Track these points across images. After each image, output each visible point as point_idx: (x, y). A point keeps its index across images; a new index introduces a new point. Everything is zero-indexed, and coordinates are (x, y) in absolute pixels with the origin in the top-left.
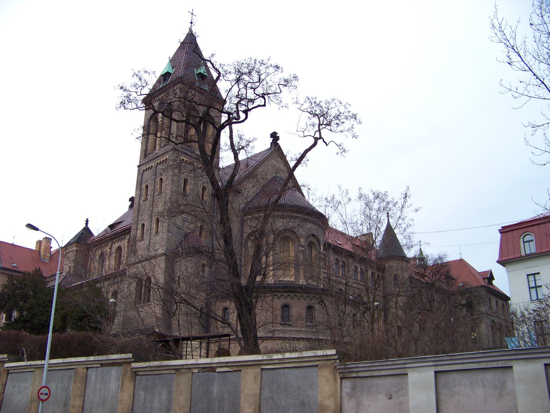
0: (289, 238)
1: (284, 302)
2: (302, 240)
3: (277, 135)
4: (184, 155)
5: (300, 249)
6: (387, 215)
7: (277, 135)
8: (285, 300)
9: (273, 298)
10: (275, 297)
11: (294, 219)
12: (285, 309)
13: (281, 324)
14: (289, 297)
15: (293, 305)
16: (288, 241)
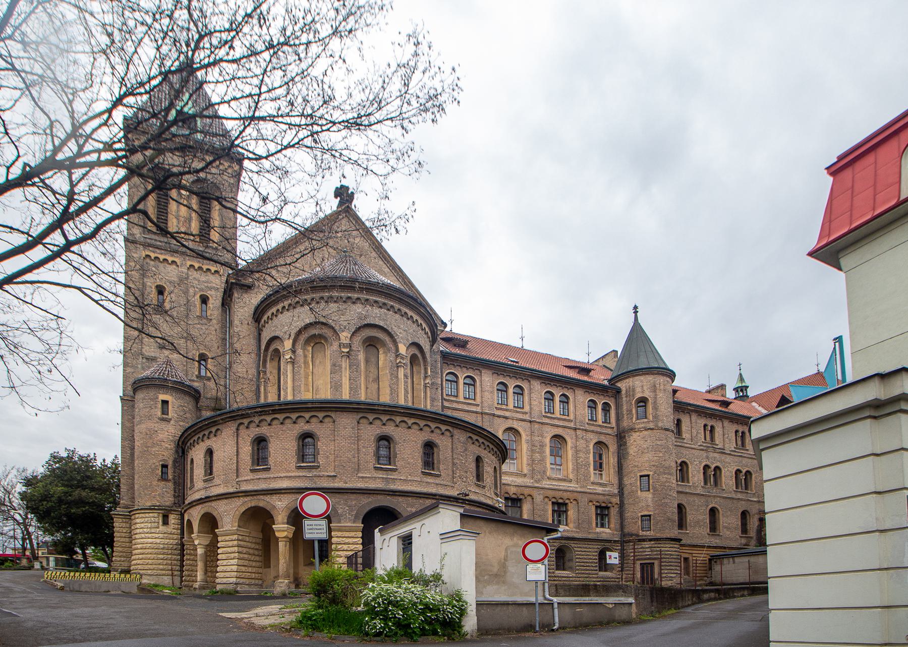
0: (321, 336)
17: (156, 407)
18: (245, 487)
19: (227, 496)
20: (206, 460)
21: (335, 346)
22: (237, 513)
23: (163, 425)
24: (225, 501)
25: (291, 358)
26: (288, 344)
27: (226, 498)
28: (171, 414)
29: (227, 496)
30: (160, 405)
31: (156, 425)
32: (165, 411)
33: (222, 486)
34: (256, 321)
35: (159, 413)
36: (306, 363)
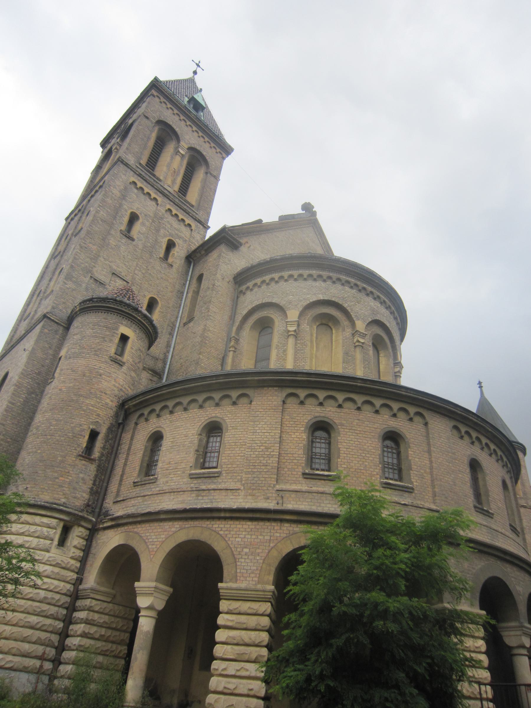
1: (317, 414)
2: (360, 326)
3: (314, 210)
4: (139, 178)
5: (355, 340)
6: (478, 385)
7: (314, 210)
8: (318, 409)
9: (284, 402)
10: (290, 400)
11: (343, 284)
12: (319, 433)
13: (306, 476)
14: (331, 402)
15: (342, 425)
16: (328, 325)
17: (111, 341)
18: (290, 505)
19: (258, 515)
20: (200, 440)
21: (348, 332)
22: (274, 553)
23: (113, 369)
24: (249, 525)
25: (295, 331)
26: (293, 315)
27: (251, 519)
28: (127, 357)
29: (258, 515)
30: (117, 340)
31: (103, 365)
32: (121, 352)
33: (242, 493)
34: (236, 283)
35: (113, 350)
36: (312, 342)
